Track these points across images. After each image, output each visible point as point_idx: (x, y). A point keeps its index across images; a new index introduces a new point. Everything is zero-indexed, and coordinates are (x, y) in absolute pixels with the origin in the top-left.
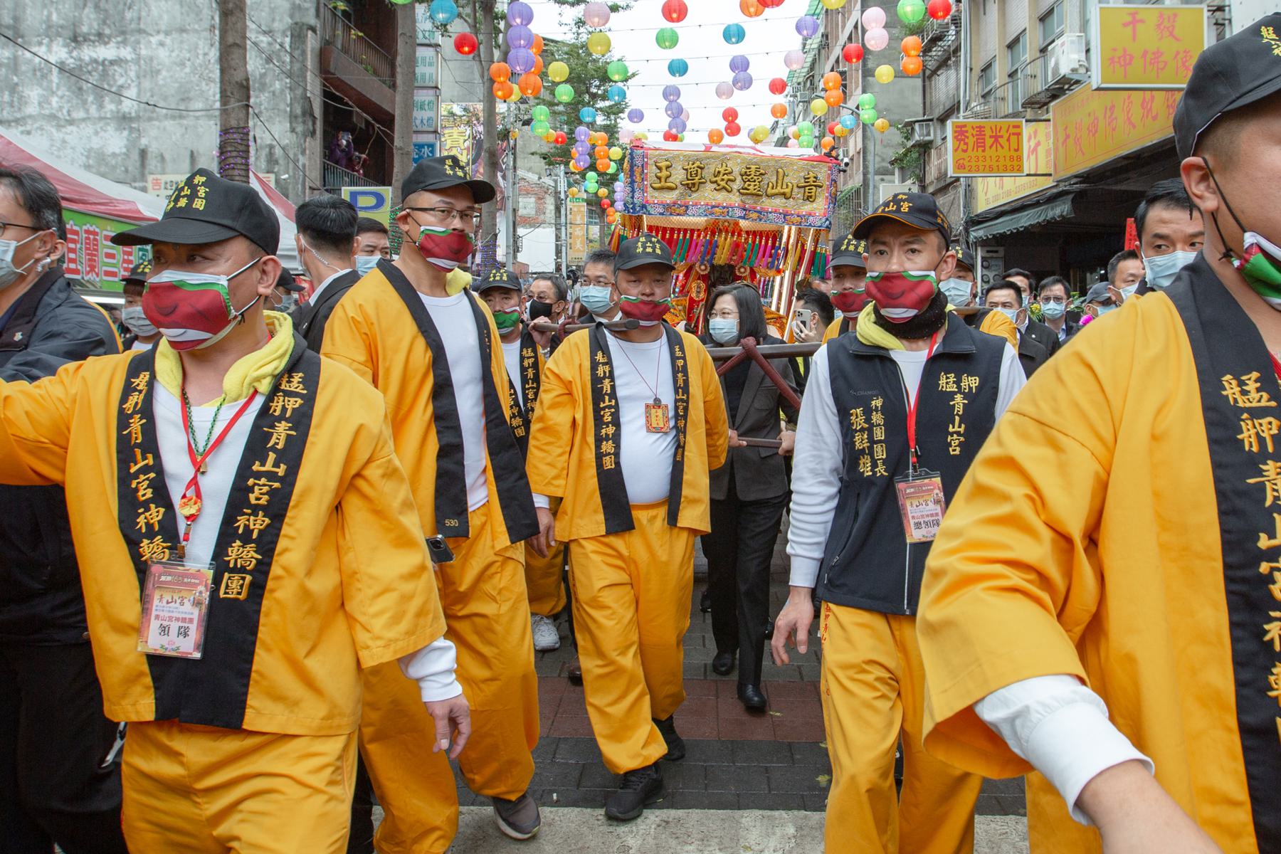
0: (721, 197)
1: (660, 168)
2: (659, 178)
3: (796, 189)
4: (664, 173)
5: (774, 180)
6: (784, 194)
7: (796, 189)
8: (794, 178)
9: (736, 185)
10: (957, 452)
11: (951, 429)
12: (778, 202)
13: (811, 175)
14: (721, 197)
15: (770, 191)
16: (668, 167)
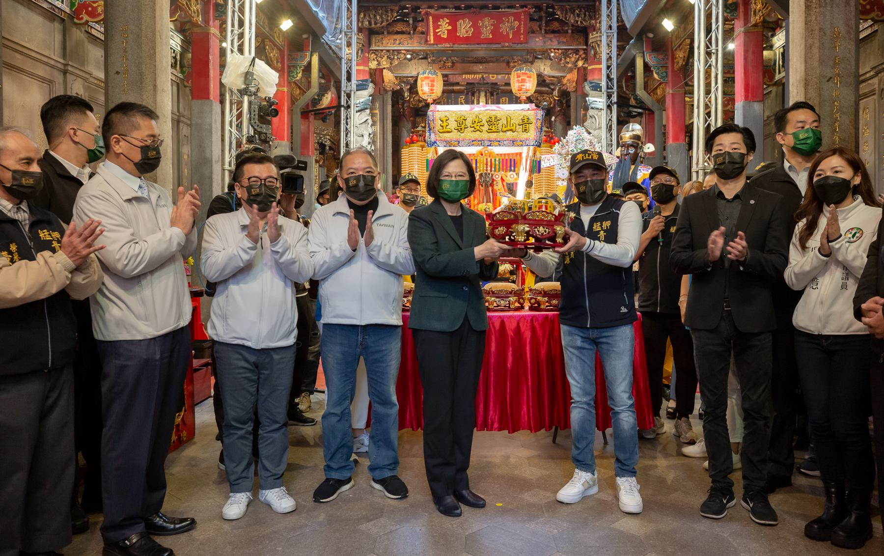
0: (477, 135)
4: (445, 124)
5: (505, 122)
8: (516, 121)
9: (486, 127)
12: (509, 133)
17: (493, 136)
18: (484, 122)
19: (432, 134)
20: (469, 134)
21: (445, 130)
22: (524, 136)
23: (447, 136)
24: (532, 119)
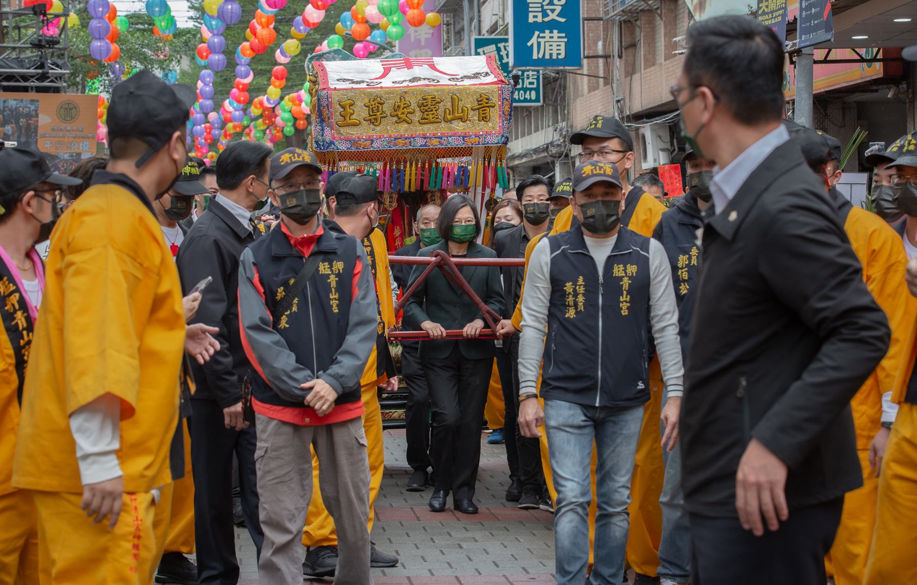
0: (403, 128)
5: (449, 105)
7: (471, 113)
8: (469, 103)
9: (418, 115)
10: (626, 313)
11: (621, 299)
12: (459, 126)
15: (449, 117)
16: (351, 105)
18: (414, 105)
19: (327, 131)
23: (354, 132)
24: (495, 100)
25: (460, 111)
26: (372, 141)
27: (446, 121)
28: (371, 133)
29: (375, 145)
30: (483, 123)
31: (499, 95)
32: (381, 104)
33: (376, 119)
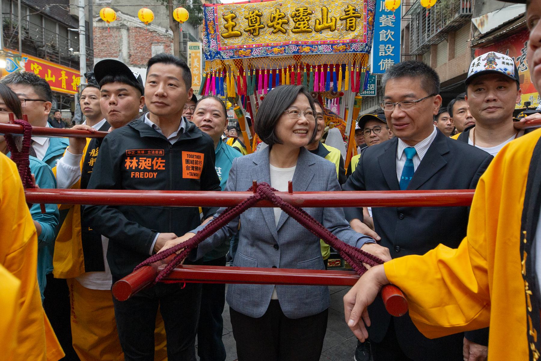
0: (280, 38)
1: (226, 20)
2: (227, 28)
3: (339, 22)
4: (231, 23)
5: (320, 17)
6: (329, 28)
7: (339, 22)
12: (327, 36)
13: (351, 8)
14: (280, 38)
15: (319, 27)
16: (233, 18)
17: (301, 38)
19: (213, 43)
20: (267, 38)
21: (230, 32)
22: (350, 36)
23: (236, 42)
25: (329, 21)
26: (252, 50)
27: (317, 31)
28: (250, 42)
29: (255, 54)
30: (350, 32)
31: (365, 8)
32: (260, 16)
33: (254, 30)
